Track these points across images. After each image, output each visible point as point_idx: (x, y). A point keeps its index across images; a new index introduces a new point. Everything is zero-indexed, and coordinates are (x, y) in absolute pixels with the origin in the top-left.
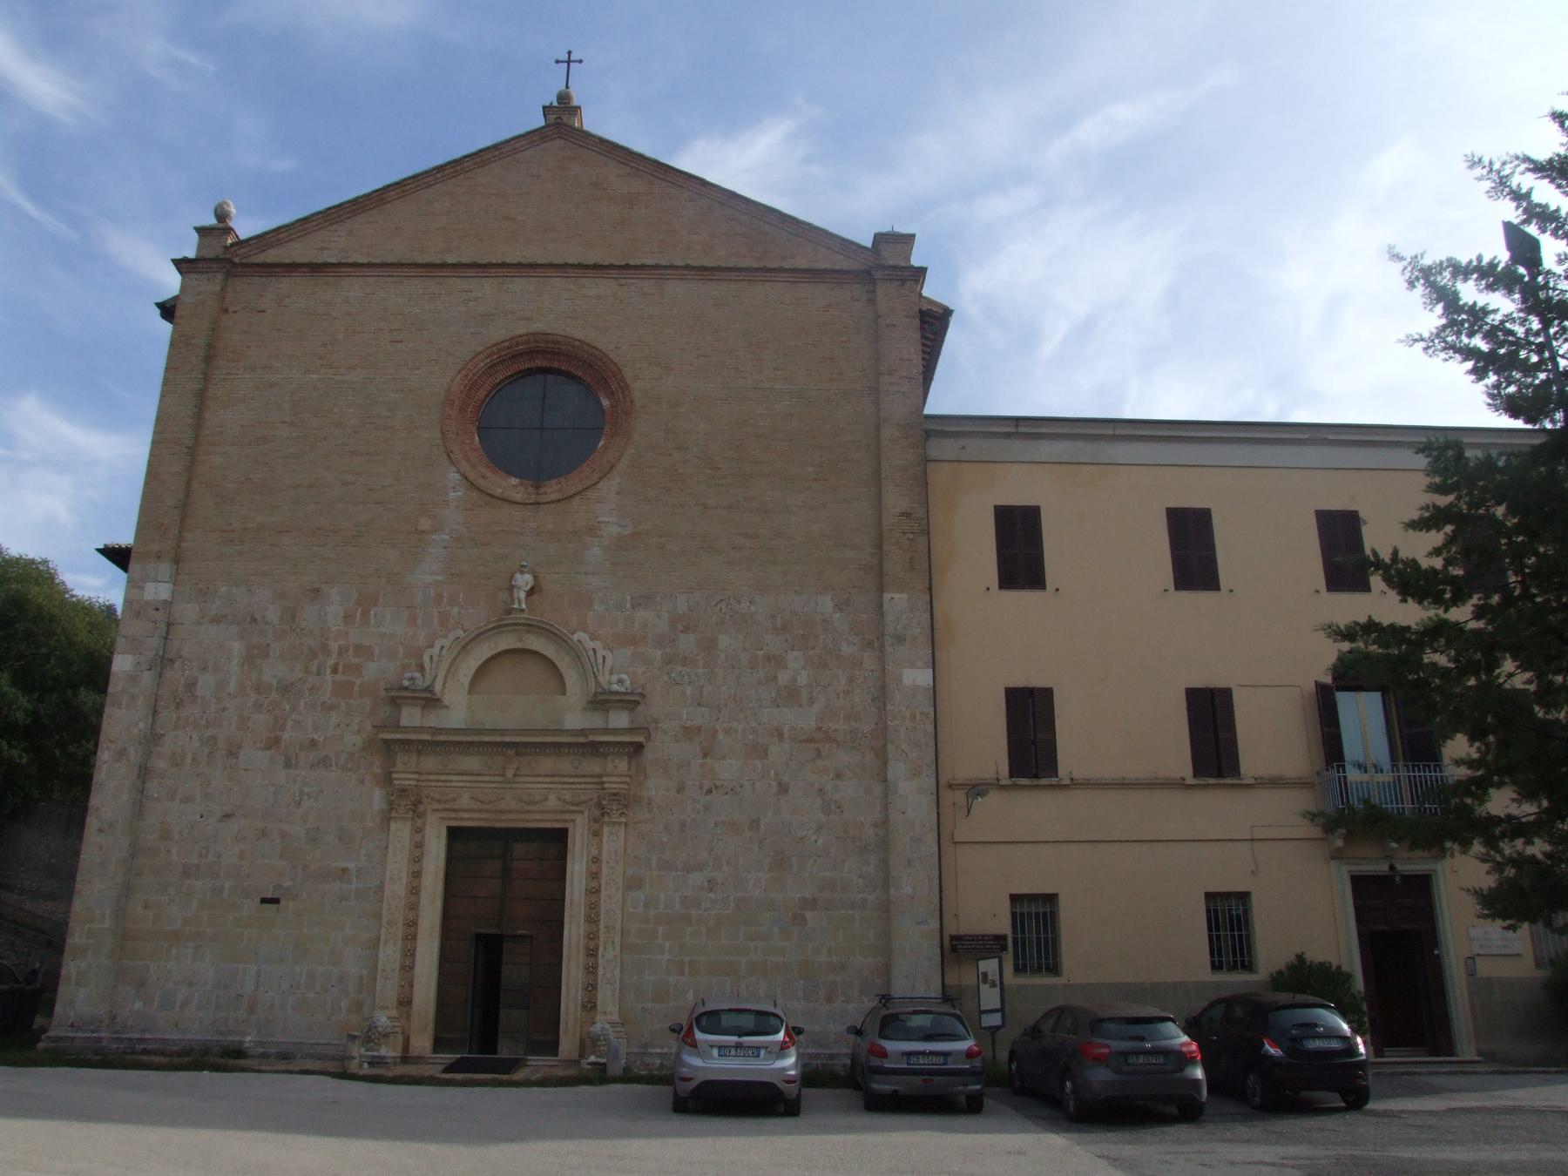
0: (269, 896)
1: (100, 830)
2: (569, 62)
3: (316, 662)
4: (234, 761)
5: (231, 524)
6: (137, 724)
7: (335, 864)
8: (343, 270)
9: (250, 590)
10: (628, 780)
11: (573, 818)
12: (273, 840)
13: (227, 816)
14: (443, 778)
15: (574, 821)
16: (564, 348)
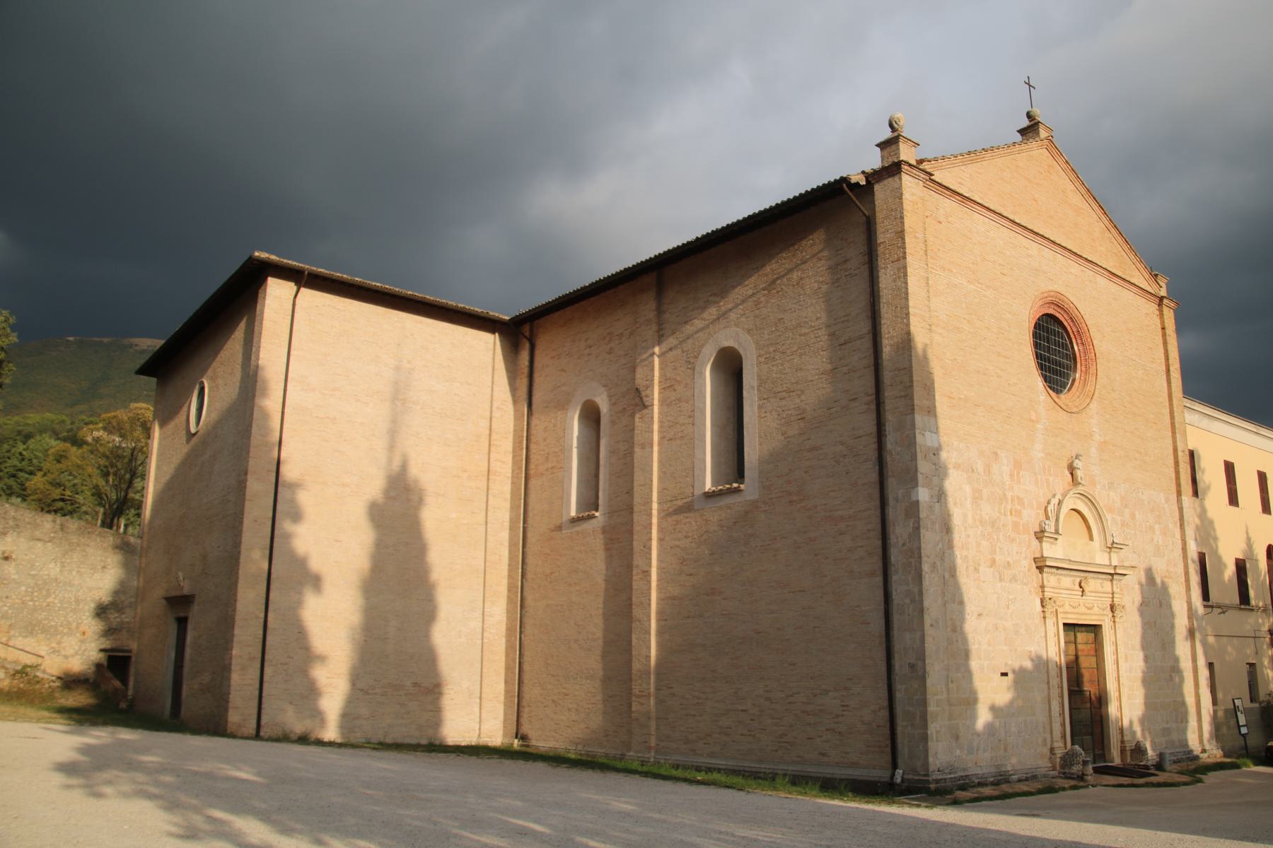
0: (1004, 671)
1: (932, 625)
2: (1030, 86)
3: (1003, 506)
4: (978, 575)
5: (952, 393)
6: (938, 544)
7: (1026, 648)
8: (977, 207)
9: (967, 447)
10: (1121, 596)
11: (1103, 618)
12: (1000, 632)
13: (980, 615)
14: (1056, 591)
15: (1104, 620)
16: (1065, 306)
